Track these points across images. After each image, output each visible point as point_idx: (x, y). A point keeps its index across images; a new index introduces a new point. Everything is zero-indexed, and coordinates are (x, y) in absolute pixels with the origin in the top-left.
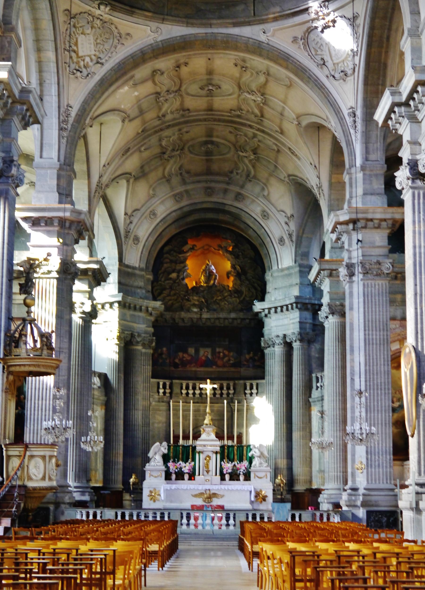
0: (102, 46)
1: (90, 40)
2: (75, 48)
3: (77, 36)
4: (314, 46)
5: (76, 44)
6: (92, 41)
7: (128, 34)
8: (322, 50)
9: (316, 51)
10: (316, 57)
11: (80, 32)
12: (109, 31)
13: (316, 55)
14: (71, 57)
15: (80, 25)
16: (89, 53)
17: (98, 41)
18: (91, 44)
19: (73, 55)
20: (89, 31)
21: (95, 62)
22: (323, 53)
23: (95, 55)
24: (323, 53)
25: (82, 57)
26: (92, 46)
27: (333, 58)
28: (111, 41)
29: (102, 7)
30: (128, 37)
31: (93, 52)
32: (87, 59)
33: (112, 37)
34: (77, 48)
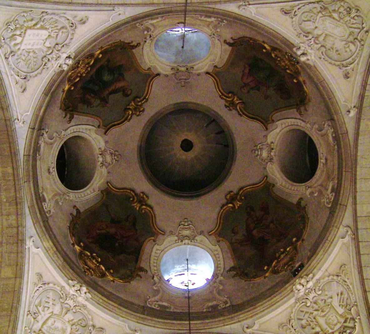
0: (24, 58)
1: (37, 44)
2: (38, 26)
3: (50, 30)
4: (43, 300)
5: (42, 28)
6: (35, 47)
7: (25, 90)
8: (43, 311)
9: (40, 304)
10: (35, 308)
11: (52, 35)
12: (37, 66)
13: (36, 306)
14: (32, 20)
15: (60, 34)
16: (24, 42)
17: (31, 54)
18: (33, 45)
19: (34, 22)
20: (47, 44)
21: (13, 49)
22: (42, 313)
23: (19, 49)
24: (42, 313)
25: (25, 33)
26: (30, 47)
27: (45, 327)
28: (25, 70)
29: (70, 62)
30: (23, 89)
31: (22, 48)
32: (19, 39)
33: (30, 70)
34: (38, 29)
